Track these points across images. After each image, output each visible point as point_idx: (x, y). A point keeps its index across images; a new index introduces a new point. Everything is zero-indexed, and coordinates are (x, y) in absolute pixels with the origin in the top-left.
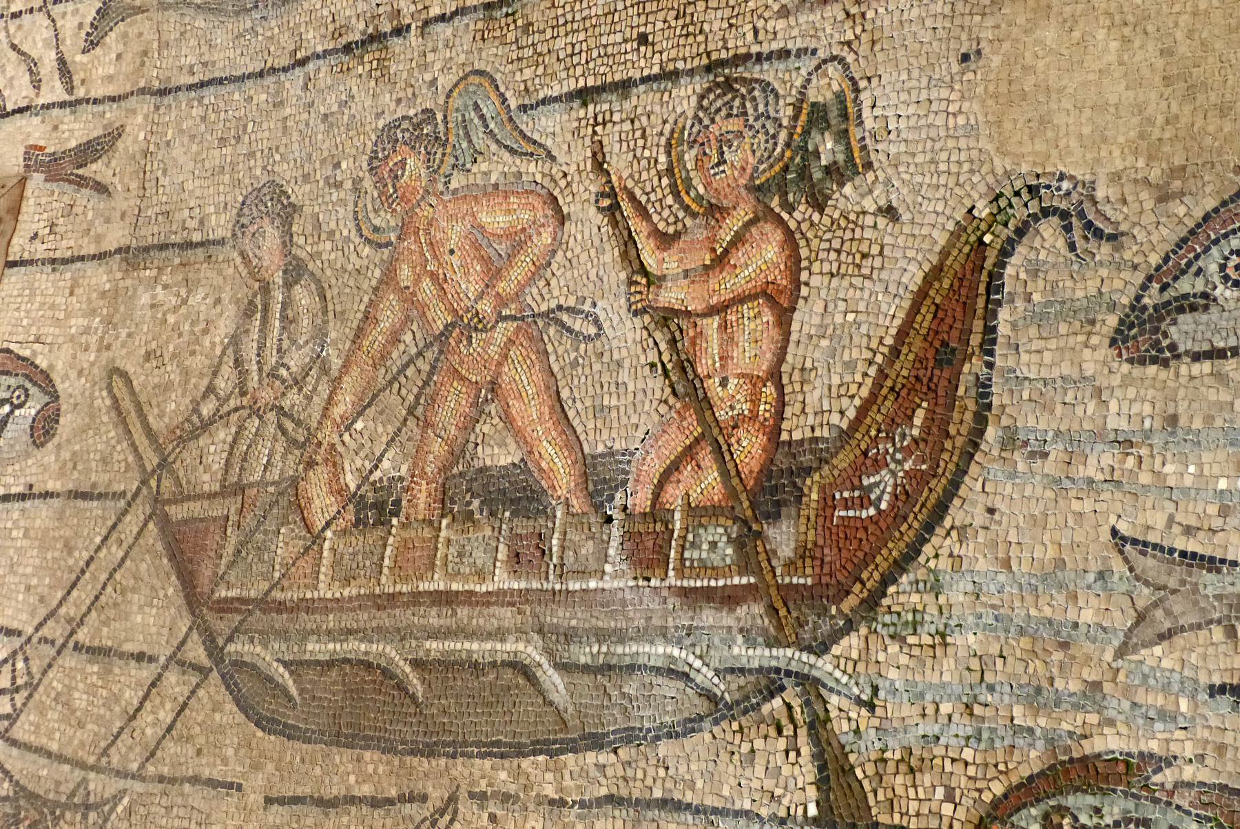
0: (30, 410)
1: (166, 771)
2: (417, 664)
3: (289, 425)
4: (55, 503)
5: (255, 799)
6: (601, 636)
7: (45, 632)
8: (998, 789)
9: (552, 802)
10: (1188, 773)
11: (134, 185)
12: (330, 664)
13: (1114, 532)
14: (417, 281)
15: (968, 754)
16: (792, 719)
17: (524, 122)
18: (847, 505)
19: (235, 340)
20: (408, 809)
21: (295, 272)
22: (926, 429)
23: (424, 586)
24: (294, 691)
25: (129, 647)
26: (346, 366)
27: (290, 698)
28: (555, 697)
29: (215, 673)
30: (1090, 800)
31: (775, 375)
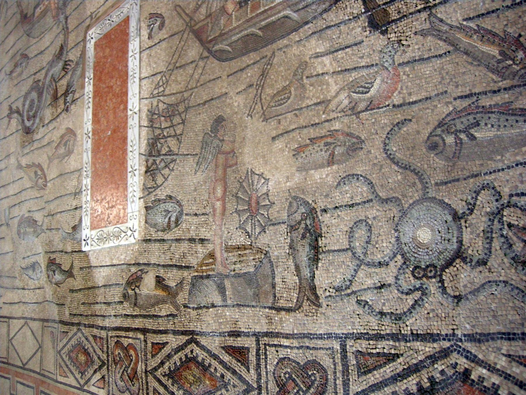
0: (158, 23)
1: (202, 83)
2: (260, 29)
4: (166, 40)
5: (224, 77)
7: (169, 68)
9: (298, 41)
12: (238, 40)
20: (263, 60)
23: (258, 12)
25: (189, 61)
27: (229, 52)
28: (295, 19)
29: (211, 57)
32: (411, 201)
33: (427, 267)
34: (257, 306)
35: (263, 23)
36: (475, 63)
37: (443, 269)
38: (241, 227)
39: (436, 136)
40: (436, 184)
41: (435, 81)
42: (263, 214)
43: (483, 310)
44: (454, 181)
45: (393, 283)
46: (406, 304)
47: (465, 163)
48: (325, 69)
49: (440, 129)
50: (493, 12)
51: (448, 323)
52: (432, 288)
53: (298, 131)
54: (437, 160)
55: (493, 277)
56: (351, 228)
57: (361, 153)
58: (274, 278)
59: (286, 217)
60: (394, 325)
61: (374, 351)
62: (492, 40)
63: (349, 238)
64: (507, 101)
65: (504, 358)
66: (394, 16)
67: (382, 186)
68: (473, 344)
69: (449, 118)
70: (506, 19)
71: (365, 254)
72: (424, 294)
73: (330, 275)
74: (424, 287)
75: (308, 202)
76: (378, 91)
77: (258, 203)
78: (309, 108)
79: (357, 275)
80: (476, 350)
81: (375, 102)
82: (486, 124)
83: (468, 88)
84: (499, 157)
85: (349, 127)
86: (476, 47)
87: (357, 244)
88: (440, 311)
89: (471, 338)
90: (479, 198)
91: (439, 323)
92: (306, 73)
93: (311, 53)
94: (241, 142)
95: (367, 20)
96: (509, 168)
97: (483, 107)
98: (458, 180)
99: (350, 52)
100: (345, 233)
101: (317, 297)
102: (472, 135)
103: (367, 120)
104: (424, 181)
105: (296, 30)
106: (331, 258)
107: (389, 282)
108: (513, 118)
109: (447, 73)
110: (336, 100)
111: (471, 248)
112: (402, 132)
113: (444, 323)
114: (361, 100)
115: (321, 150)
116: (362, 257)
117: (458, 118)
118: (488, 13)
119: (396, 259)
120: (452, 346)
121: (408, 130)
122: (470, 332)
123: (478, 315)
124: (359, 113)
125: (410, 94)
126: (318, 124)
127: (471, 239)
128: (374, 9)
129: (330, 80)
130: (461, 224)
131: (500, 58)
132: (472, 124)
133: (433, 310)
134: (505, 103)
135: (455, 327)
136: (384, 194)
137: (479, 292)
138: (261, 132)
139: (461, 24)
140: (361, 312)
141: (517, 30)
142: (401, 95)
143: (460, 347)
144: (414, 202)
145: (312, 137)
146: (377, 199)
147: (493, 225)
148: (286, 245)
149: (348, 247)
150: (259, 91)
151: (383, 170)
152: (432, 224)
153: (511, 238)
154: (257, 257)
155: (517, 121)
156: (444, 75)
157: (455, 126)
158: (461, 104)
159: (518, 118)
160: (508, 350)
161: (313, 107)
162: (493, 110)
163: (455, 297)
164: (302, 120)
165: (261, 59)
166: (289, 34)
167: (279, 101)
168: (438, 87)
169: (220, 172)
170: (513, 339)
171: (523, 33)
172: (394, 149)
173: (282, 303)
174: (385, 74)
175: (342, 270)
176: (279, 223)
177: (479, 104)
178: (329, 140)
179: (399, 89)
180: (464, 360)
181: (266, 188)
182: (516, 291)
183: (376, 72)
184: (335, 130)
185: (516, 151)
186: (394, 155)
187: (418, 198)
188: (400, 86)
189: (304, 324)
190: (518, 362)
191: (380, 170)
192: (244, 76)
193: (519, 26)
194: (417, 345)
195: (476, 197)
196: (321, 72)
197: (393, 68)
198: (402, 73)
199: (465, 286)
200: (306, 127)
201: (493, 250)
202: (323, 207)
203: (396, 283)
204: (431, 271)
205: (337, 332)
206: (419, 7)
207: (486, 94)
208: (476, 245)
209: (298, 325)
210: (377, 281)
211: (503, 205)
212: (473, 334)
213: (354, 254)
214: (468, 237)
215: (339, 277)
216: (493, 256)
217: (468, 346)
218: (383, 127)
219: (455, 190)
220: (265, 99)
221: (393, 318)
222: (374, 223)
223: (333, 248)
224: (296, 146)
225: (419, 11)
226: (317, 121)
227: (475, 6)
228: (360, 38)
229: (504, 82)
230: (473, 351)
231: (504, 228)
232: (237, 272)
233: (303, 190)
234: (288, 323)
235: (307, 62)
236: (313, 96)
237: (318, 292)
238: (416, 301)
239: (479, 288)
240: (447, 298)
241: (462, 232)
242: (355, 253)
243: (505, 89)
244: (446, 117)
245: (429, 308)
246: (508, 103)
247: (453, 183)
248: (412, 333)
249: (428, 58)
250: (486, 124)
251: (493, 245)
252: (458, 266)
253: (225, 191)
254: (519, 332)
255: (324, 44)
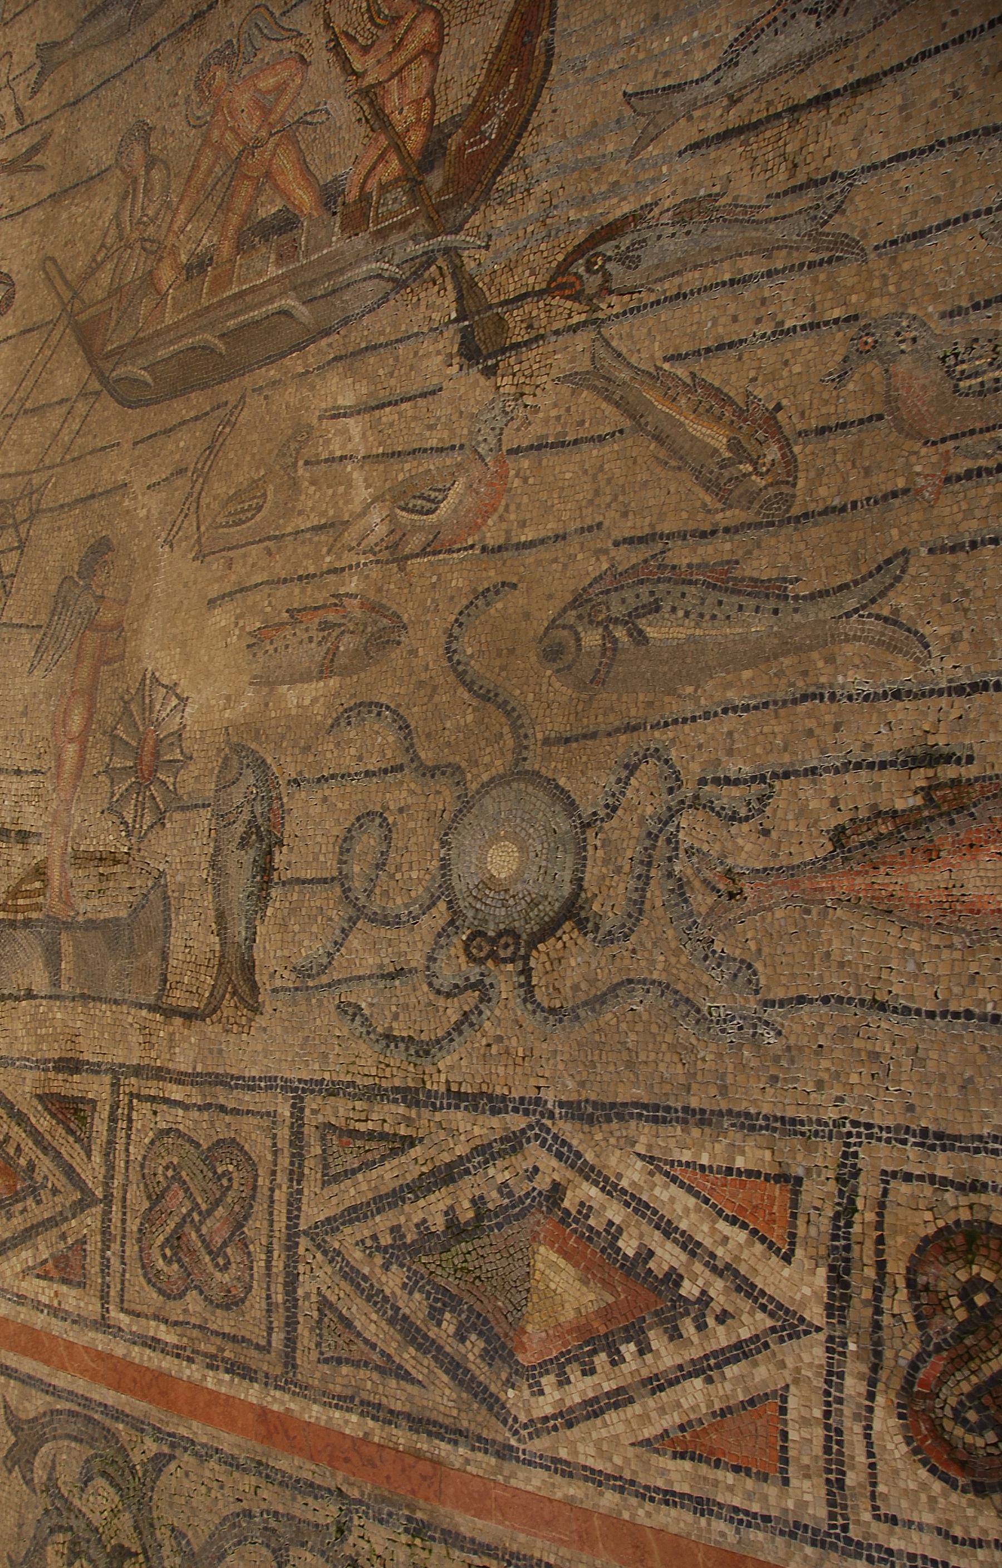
2: (222, 336)
3: (148, 245)
6: (329, 276)
8: (560, 257)
10: (667, 204)
11: (58, 160)
13: (625, 94)
14: (222, 135)
15: (543, 247)
16: (442, 275)
17: (285, 22)
18: (472, 145)
19: (117, 215)
21: (151, 163)
22: (517, 82)
24: (150, 380)
26: (181, 201)
28: (303, 319)
30: (613, 243)
31: (431, 94)
32: (485, 777)
33: (500, 934)
34: (124, 1001)
35: (231, 323)
36: (673, 463)
37: (533, 944)
38: (113, 810)
39: (564, 627)
40: (547, 741)
41: (581, 496)
42: (164, 783)
43: (607, 1048)
44: (585, 736)
45: (421, 968)
46: (444, 1019)
47: (615, 697)
48: (350, 447)
49: (574, 613)
50: (731, 345)
51: (528, 1071)
52: (503, 987)
53: (266, 590)
54: (557, 685)
55: (638, 969)
56: (349, 831)
57: (395, 654)
58: (167, 935)
59: (212, 794)
60: (411, 1068)
61: (362, 1127)
62: (717, 410)
63: (341, 853)
64: (726, 557)
65: (639, 1164)
66: (519, 334)
67: (428, 736)
68: (578, 1125)
69: (597, 589)
70: (755, 364)
71: (369, 893)
72: (485, 999)
73: (288, 937)
74: (487, 981)
75: (264, 761)
76: (455, 511)
77: (156, 755)
78: (301, 537)
79: (346, 943)
80: (581, 1142)
81: (446, 536)
82: (674, 610)
83: (648, 520)
84: (690, 689)
85: (380, 590)
86: (682, 424)
87: (356, 869)
88: (514, 1041)
89: (574, 1110)
90: (633, 781)
91: (510, 1070)
92: (307, 453)
93: (323, 405)
94: (141, 605)
95: (458, 338)
96: (706, 715)
97: (674, 567)
98: (594, 735)
99: (410, 413)
100: (332, 840)
101: (254, 988)
102: (640, 632)
103: (421, 576)
104: (522, 731)
105: (299, 347)
106: (295, 897)
107: (413, 964)
108: (735, 599)
109: (609, 481)
110: (363, 522)
111: (599, 899)
112: (493, 611)
113: (519, 1070)
114: (416, 529)
115: (311, 639)
116: (362, 898)
117: (616, 589)
118: (720, 347)
119: (434, 911)
120: (531, 1127)
121: (505, 608)
122: (574, 1097)
123: (596, 1058)
124: (407, 558)
125: (523, 524)
126: (314, 576)
127: (604, 878)
128: (478, 313)
129: (355, 475)
130: (585, 840)
131: (727, 455)
132: (644, 606)
133: (499, 1039)
134: (722, 563)
135: (542, 1083)
136: (430, 754)
137: (603, 1003)
138: (186, 585)
139: (657, 368)
140: (345, 1032)
141: (775, 394)
142: (504, 526)
143: (548, 1131)
144: (492, 780)
145: (296, 605)
146: (414, 765)
147: (654, 847)
148: (203, 858)
149: (336, 874)
150: (198, 486)
151: (437, 699)
152: (523, 834)
153: (689, 882)
154: (138, 883)
155: (741, 608)
156: (602, 484)
157: (608, 609)
158: (629, 557)
159: (744, 601)
160: (649, 1147)
161: (308, 535)
162: (695, 578)
163: (552, 1011)
164: (278, 565)
165: (213, 410)
166: (283, 355)
167: (236, 513)
168: (584, 512)
169: (84, 672)
170: (664, 1121)
171: (785, 402)
172: (469, 651)
173: (179, 998)
174: (476, 470)
175: (315, 929)
176: (196, 806)
177: (666, 562)
178: (331, 617)
179: (501, 509)
180: (554, 1163)
181: (178, 720)
182: (684, 1008)
183: (459, 465)
184: (347, 595)
185: (729, 678)
186: (467, 664)
187: (501, 770)
188: (503, 503)
189: (220, 1051)
190: (667, 1174)
191: (431, 697)
192: (171, 447)
193: (781, 384)
194: (460, 1118)
195: (628, 778)
196: (338, 454)
197: (496, 460)
198: (512, 473)
199: (575, 988)
200: (285, 581)
201: (647, 906)
202: (294, 776)
203: (428, 968)
204: (506, 946)
205: (288, 1075)
206: (576, 319)
207: (684, 538)
208: (612, 892)
209: (206, 1053)
210: (386, 961)
211: (682, 802)
212: (579, 1102)
213: (346, 891)
214: (595, 871)
215: (306, 943)
216: (646, 922)
217: (566, 1128)
218: (452, 598)
219: (584, 758)
220: (208, 505)
221: (412, 1051)
222: (399, 821)
223: (303, 875)
224: (258, 625)
225: (574, 329)
226: (311, 570)
227: (695, 328)
228: (435, 381)
229: (728, 513)
230: (575, 1143)
231: (677, 856)
232: (89, 915)
233: (257, 731)
234: (186, 1045)
235: (309, 425)
236: (312, 509)
237: (257, 978)
238: (465, 1014)
239: (605, 994)
240: (534, 1012)
241: (585, 858)
242: (349, 889)
243: (727, 530)
244: (590, 585)
245: (491, 1033)
246: (728, 562)
247: (582, 742)
248: (449, 1090)
249: (576, 442)
250: (674, 610)
251: (648, 895)
252: (566, 937)
253: (89, 720)
254: (679, 1105)
255: (357, 386)
